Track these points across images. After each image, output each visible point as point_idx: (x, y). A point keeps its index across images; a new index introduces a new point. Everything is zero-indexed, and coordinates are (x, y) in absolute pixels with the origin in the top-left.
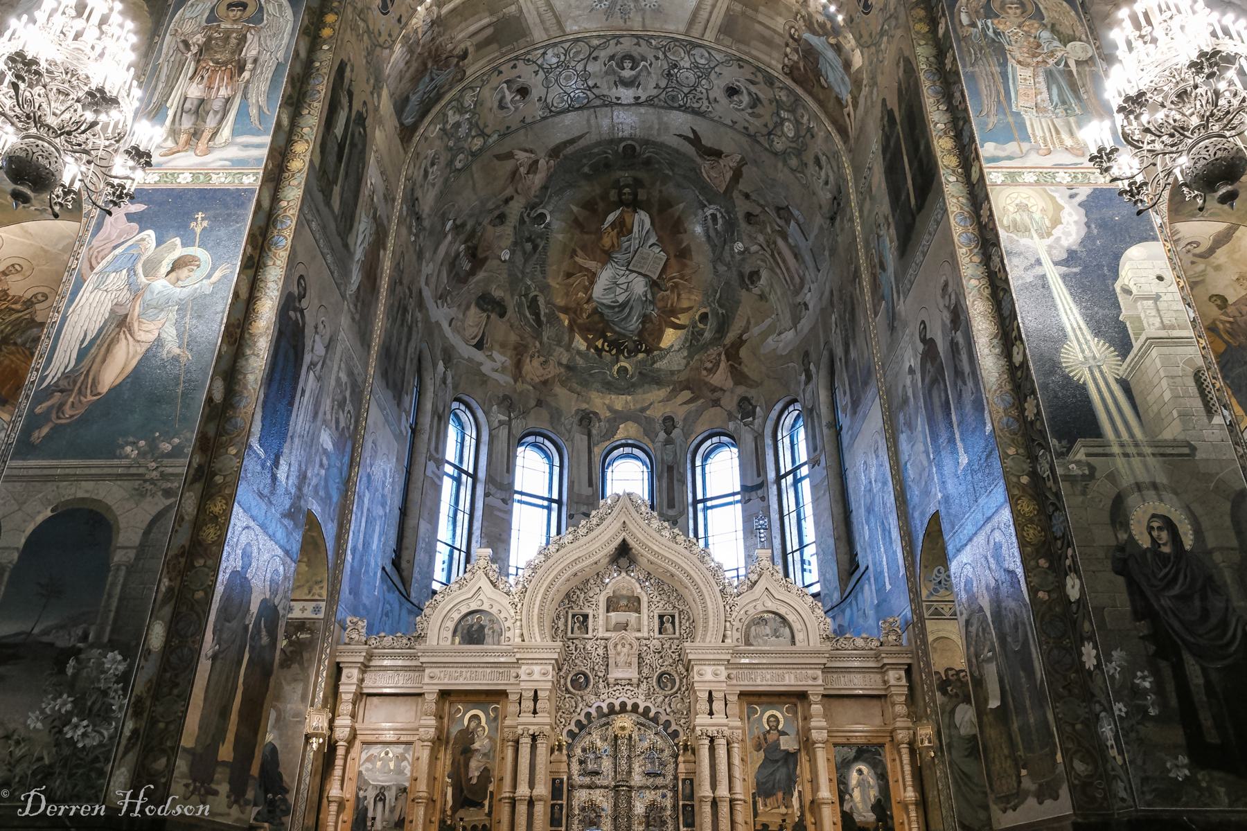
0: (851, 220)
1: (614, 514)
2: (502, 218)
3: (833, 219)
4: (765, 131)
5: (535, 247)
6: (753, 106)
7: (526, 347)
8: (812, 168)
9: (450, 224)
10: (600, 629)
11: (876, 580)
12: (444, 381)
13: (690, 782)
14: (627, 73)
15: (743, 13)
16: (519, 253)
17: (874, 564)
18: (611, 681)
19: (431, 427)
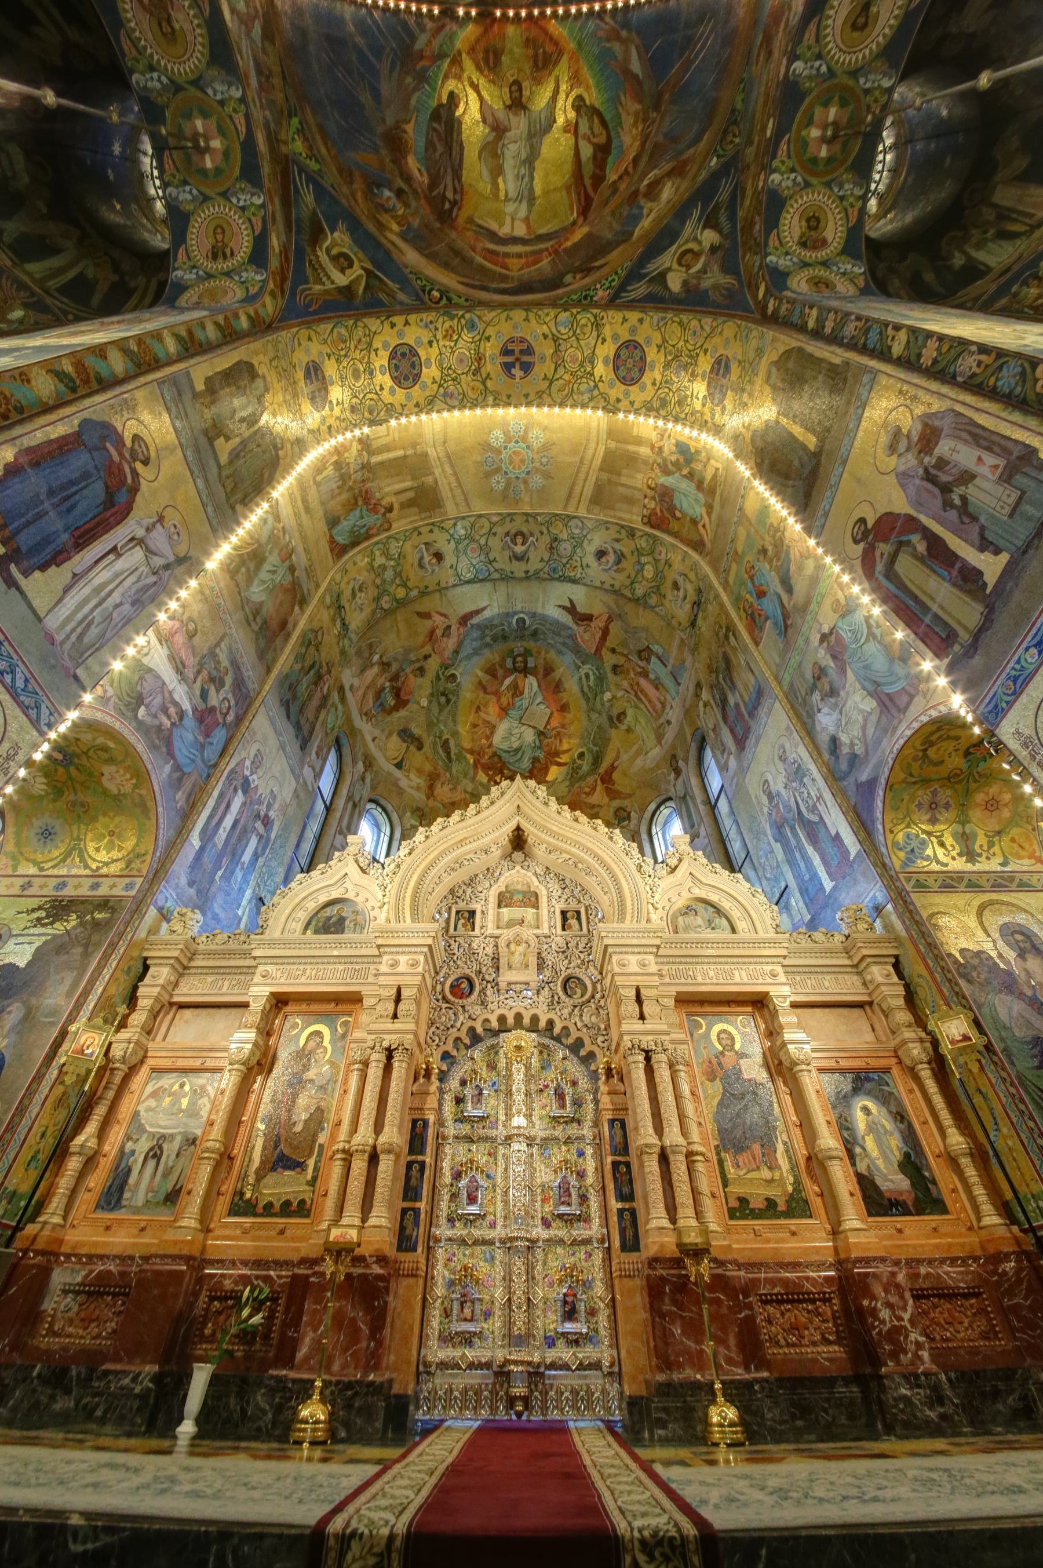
0: (717, 596)
1: (507, 796)
2: (421, 671)
3: (693, 624)
4: (628, 582)
5: (448, 701)
6: (618, 562)
7: (438, 776)
8: (670, 594)
9: (376, 658)
10: (490, 925)
11: (804, 892)
12: (363, 779)
13: (619, 1123)
14: (519, 549)
15: (609, 481)
16: (435, 704)
17: (798, 877)
18: (503, 985)
19: (345, 809)
